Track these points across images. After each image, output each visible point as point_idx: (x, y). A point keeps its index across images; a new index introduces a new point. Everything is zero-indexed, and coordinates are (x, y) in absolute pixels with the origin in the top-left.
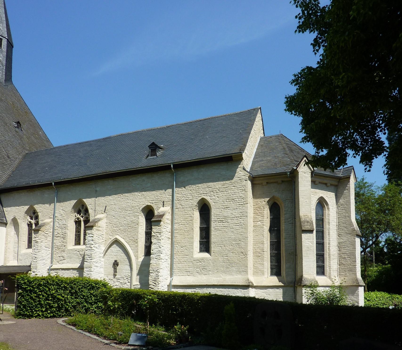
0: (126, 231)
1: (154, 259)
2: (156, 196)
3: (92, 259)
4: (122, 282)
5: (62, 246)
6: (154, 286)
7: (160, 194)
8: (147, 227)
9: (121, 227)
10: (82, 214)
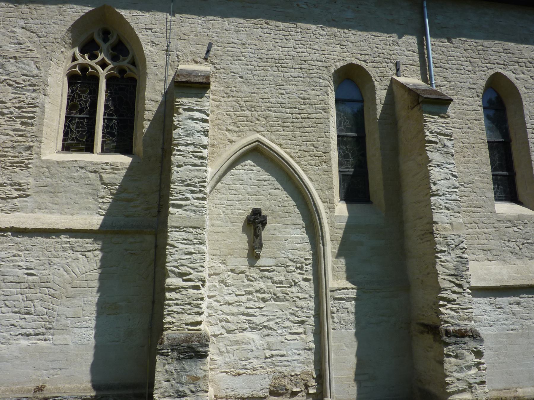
0: (286, 124)
1: (441, 209)
3: (204, 199)
4: (282, 278)
5: (14, 147)
6: (454, 292)
7: (385, 44)
10: (101, 57)
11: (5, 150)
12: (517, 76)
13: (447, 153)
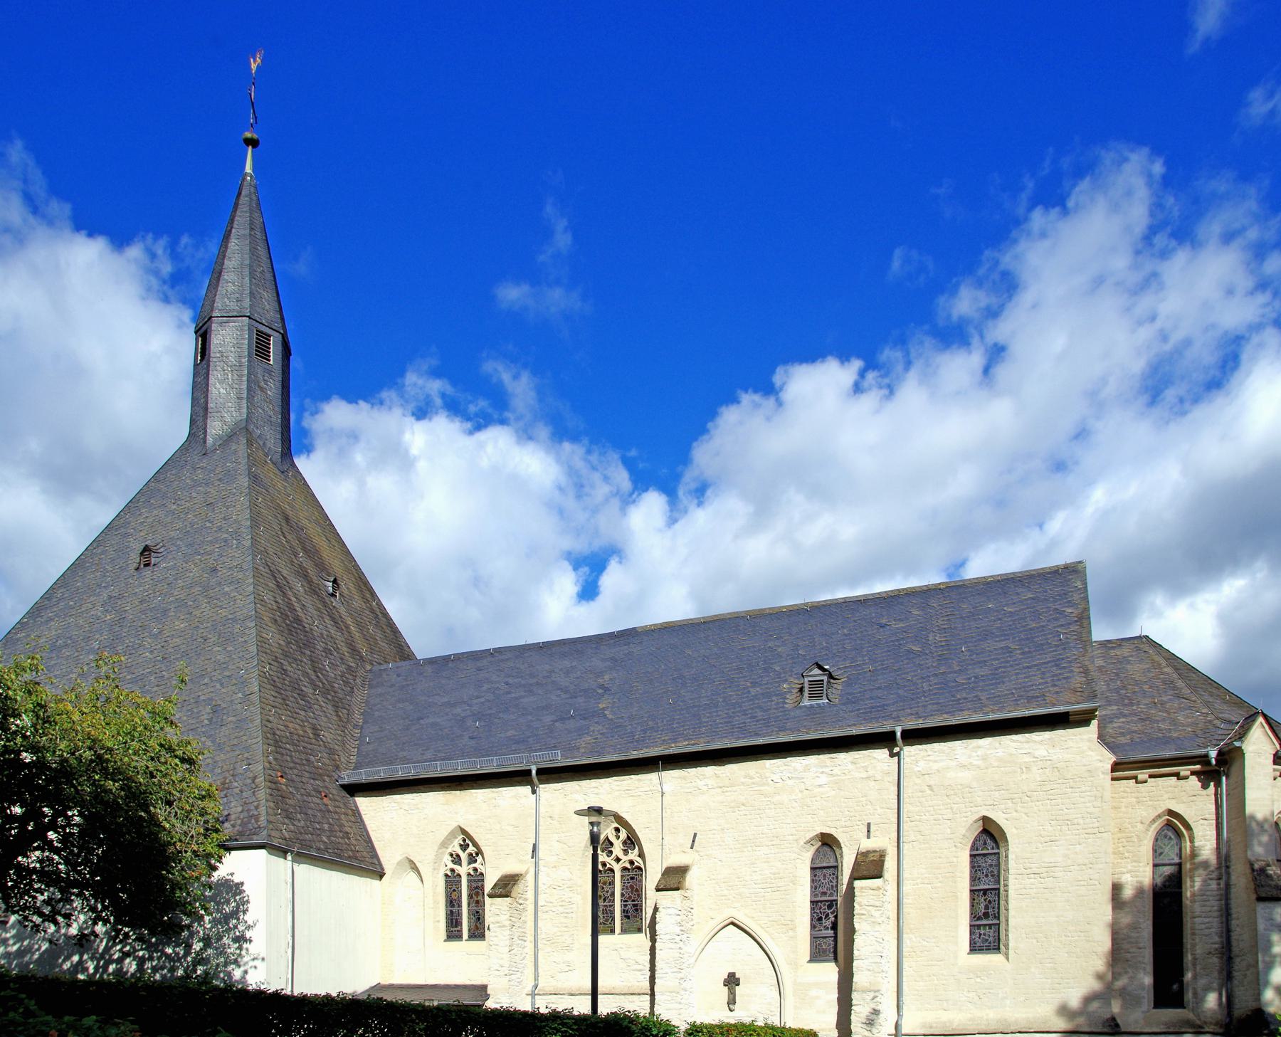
0: (758, 899)
1: (862, 971)
2: (846, 809)
7: (858, 806)
13: (874, 922)
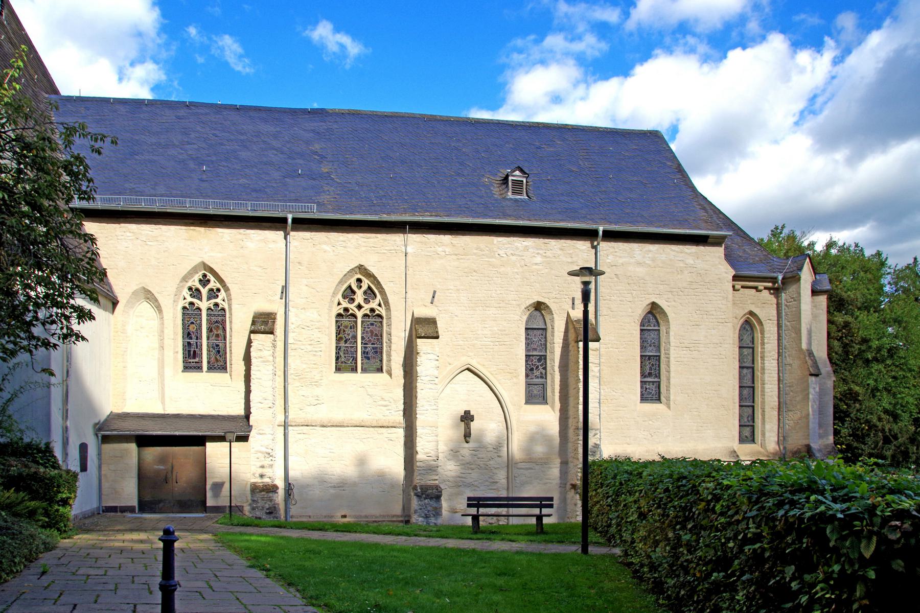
7: (565, 283)
8: (528, 345)
9: (476, 342)
11: (306, 374)
12: (669, 304)
